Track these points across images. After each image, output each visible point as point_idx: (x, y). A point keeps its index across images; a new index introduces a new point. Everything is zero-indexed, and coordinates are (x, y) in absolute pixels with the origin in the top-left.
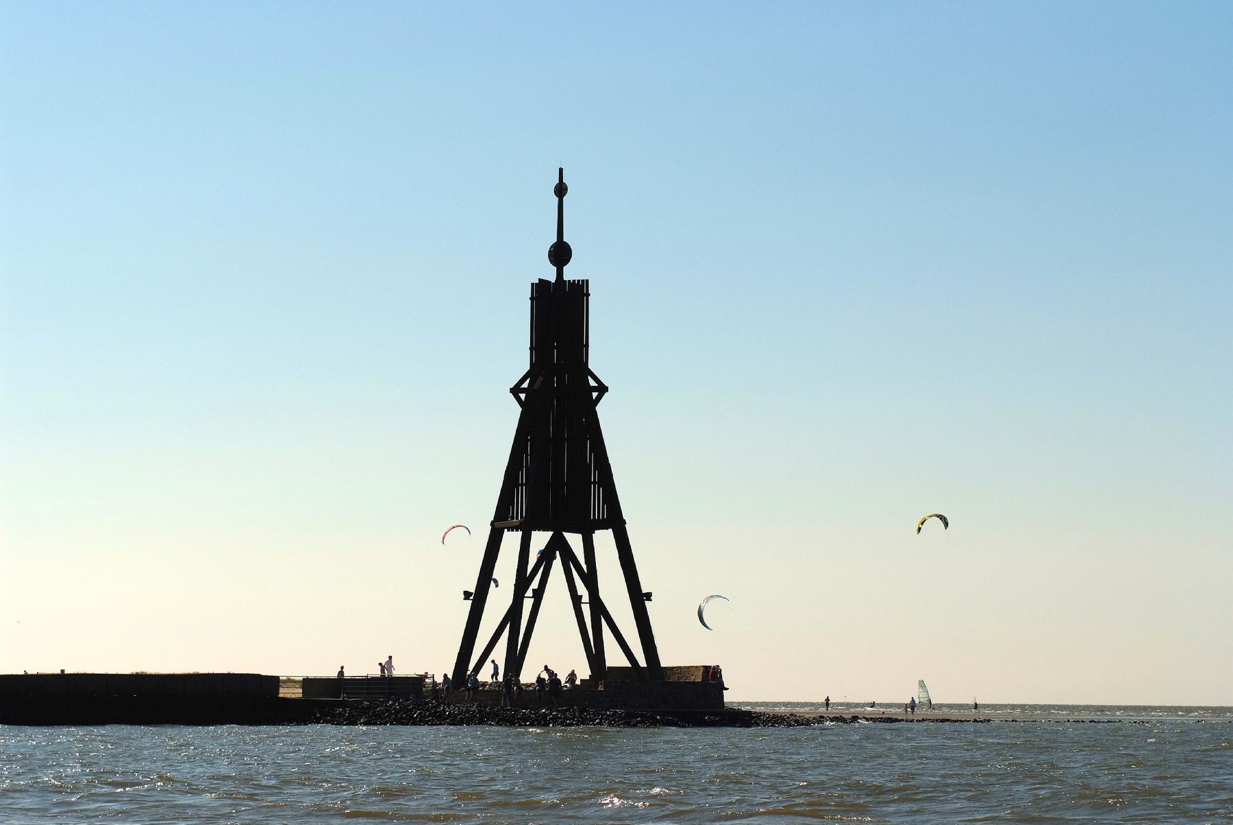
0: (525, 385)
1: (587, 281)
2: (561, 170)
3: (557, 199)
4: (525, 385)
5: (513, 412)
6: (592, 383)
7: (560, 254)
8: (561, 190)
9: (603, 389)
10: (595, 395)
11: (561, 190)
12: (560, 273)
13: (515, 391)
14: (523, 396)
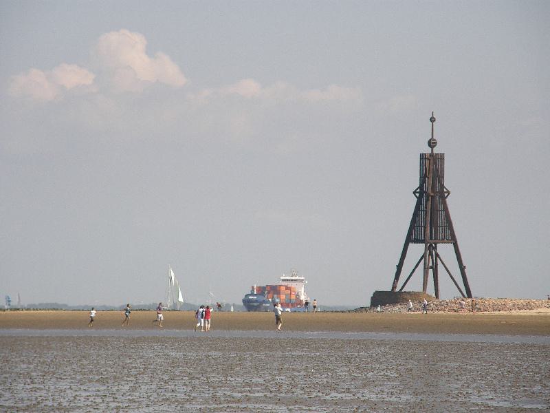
0: (418, 190)
4: (418, 190)
6: (445, 190)
7: (432, 143)
8: (433, 120)
9: (448, 193)
10: (446, 195)
11: (433, 120)
12: (432, 150)
13: (415, 193)
14: (418, 195)
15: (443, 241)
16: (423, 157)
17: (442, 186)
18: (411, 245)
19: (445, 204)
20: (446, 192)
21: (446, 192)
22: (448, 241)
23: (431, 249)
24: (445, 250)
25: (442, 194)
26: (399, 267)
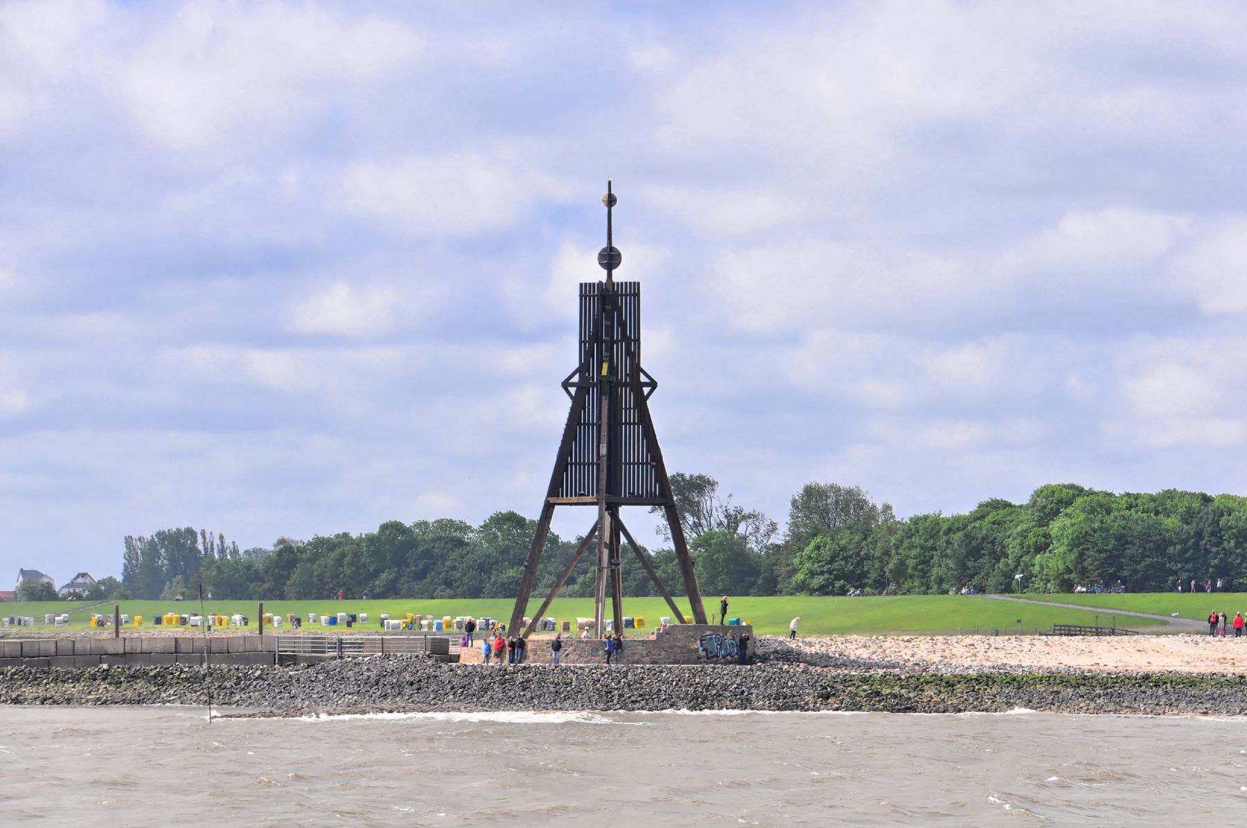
1: (639, 283)
2: (610, 183)
3: (606, 209)
4: (576, 379)
5: (563, 406)
6: (643, 379)
7: (610, 258)
8: (611, 201)
9: (653, 385)
10: (646, 390)
11: (611, 201)
12: (610, 275)
13: (566, 385)
14: (573, 390)
15: (636, 500)
16: (586, 291)
17: (636, 369)
20: (646, 385)
21: (646, 385)
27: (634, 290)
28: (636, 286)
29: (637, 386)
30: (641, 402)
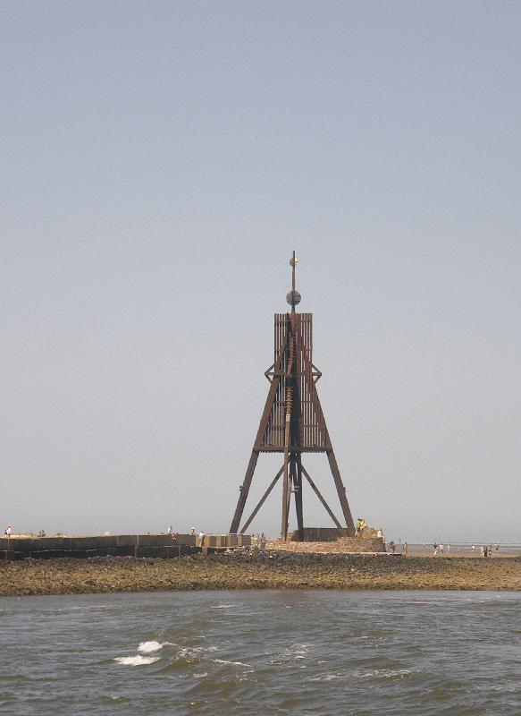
5: (265, 387)
6: (313, 371)
7: (294, 299)
8: (293, 264)
10: (315, 377)
11: (293, 264)
12: (294, 308)
14: (271, 377)
18: (263, 457)
19: (313, 390)
20: (314, 374)
22: (322, 450)
23: (294, 459)
24: (313, 462)
25: (312, 377)
26: (244, 492)
27: (308, 318)
28: (309, 316)
29: (309, 375)
30: (312, 385)
